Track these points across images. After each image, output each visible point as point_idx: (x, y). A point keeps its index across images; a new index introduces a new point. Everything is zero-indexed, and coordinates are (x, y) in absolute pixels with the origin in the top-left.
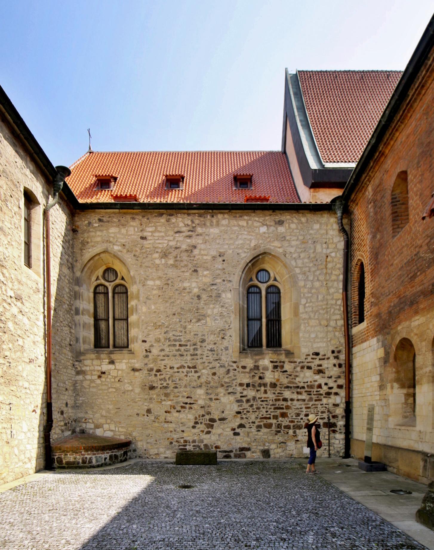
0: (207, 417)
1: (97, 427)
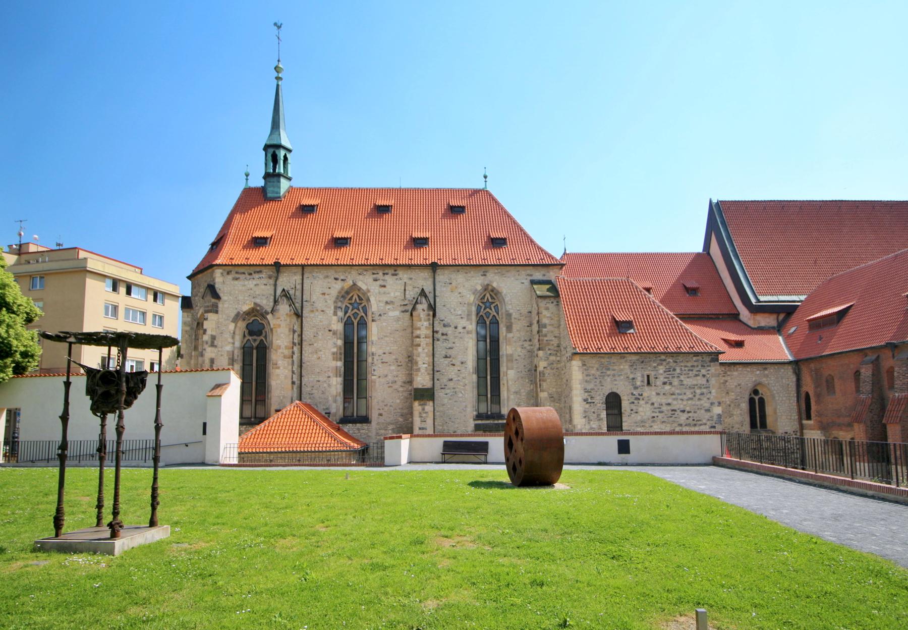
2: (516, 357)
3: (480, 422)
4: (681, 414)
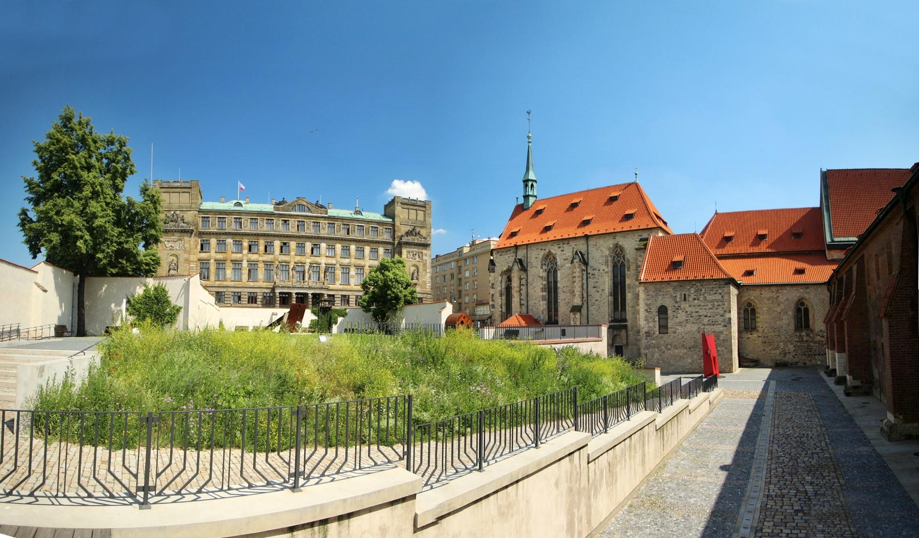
2: (632, 285)
3: (612, 324)
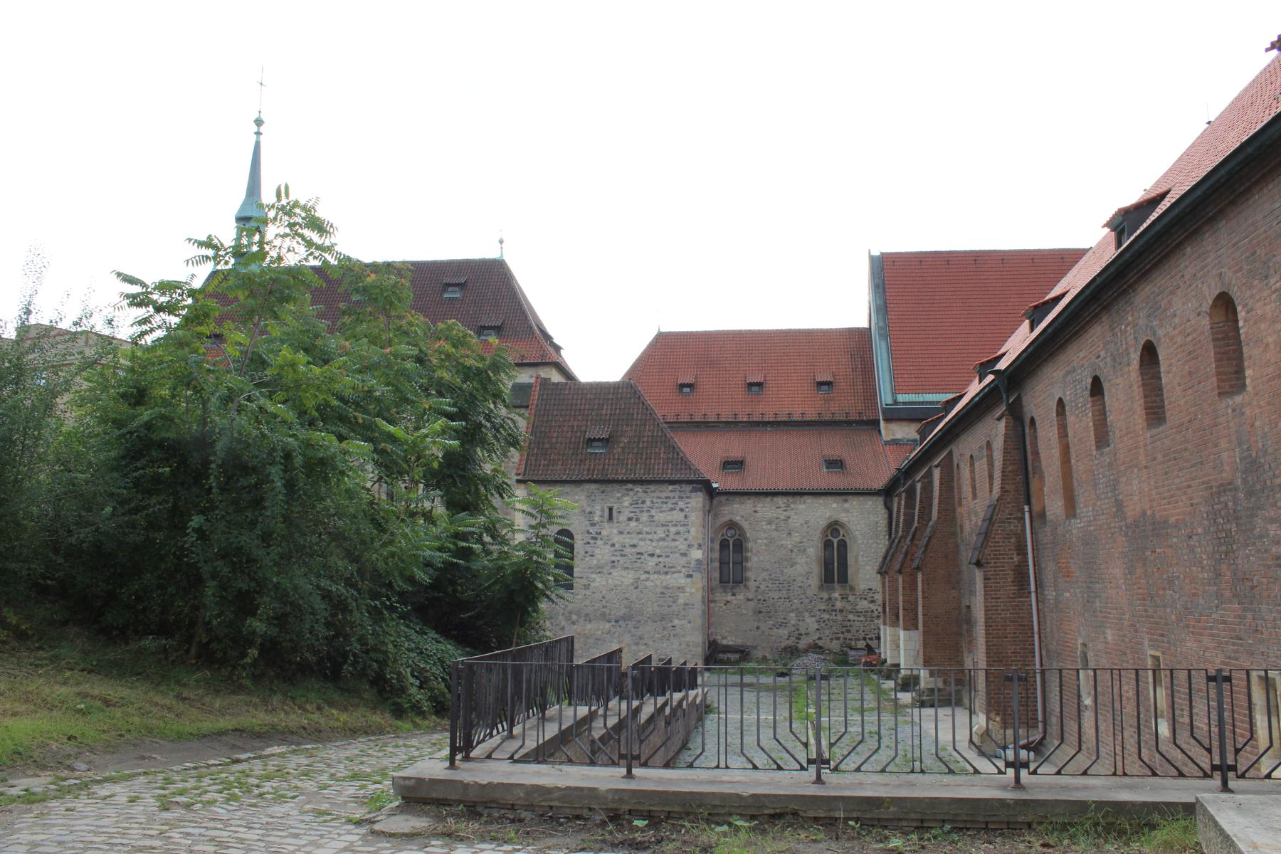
0: (797, 632)
1: (724, 638)
4: (649, 558)
